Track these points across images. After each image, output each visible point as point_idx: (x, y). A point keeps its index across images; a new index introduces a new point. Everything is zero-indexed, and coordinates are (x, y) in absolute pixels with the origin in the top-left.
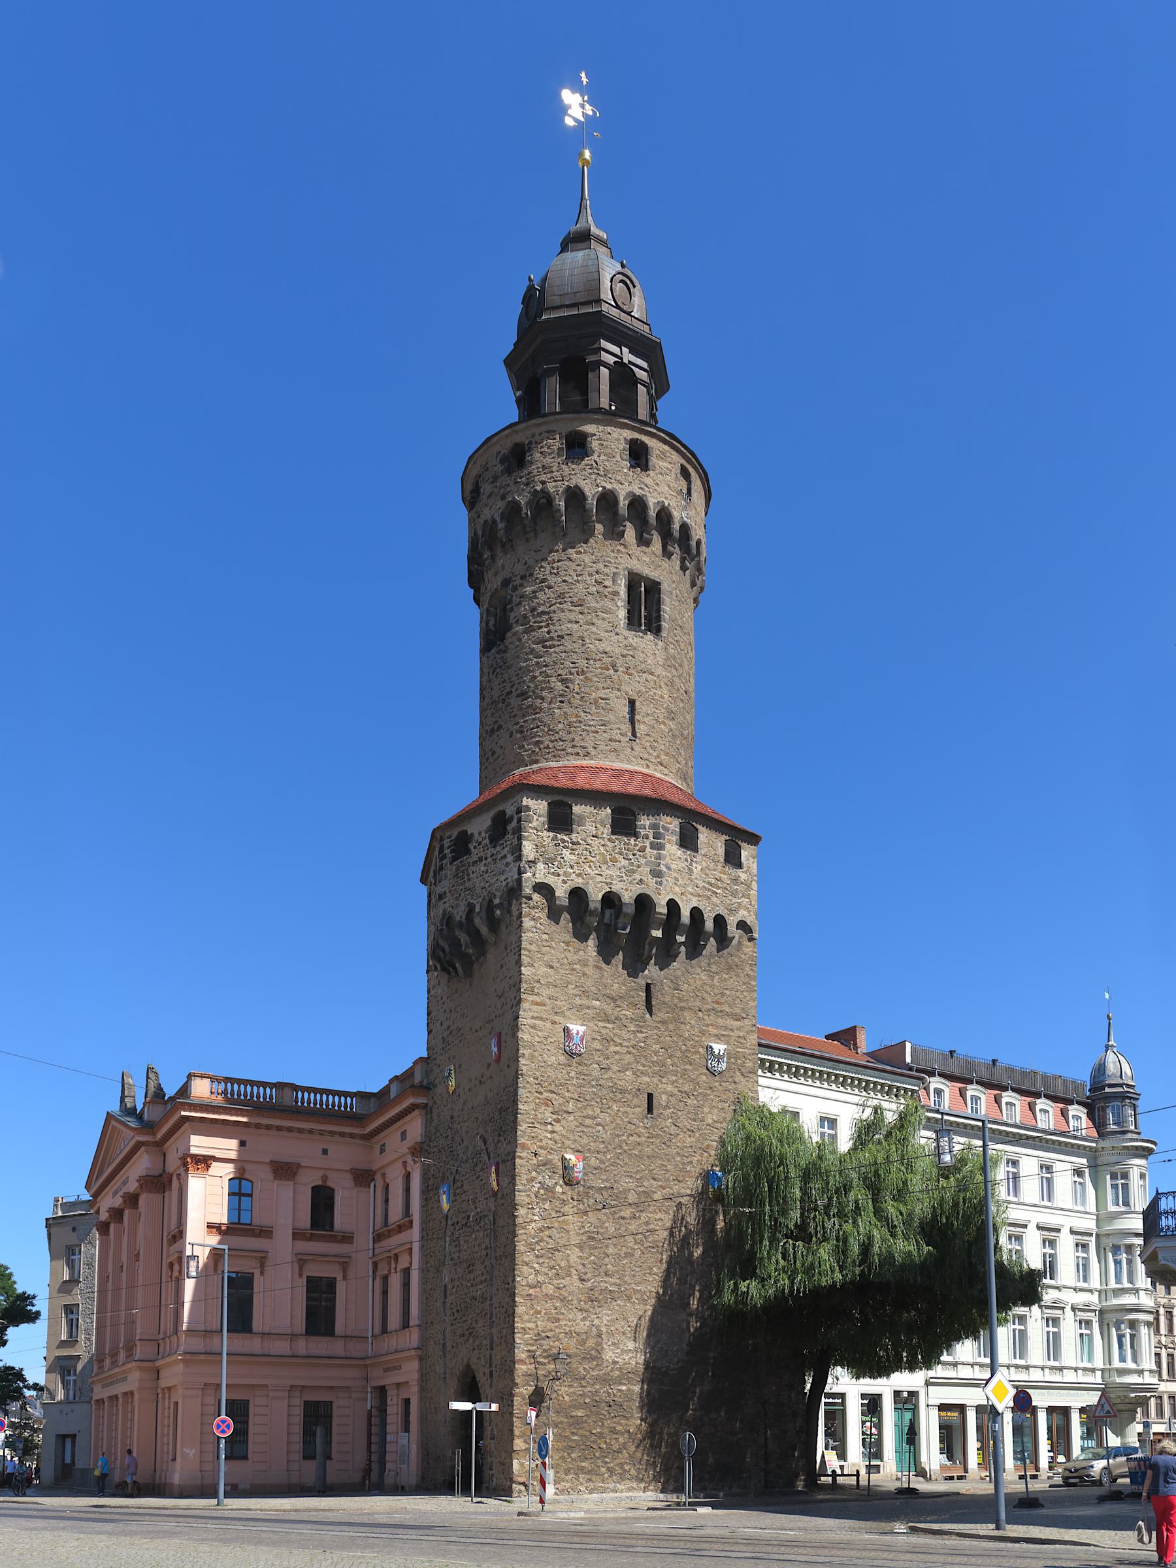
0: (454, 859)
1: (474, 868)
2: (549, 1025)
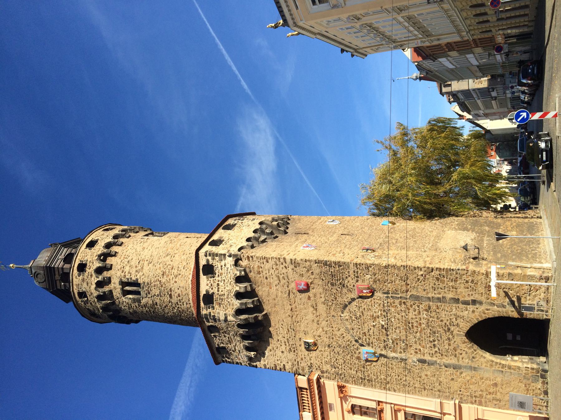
0: (213, 308)
1: (220, 290)
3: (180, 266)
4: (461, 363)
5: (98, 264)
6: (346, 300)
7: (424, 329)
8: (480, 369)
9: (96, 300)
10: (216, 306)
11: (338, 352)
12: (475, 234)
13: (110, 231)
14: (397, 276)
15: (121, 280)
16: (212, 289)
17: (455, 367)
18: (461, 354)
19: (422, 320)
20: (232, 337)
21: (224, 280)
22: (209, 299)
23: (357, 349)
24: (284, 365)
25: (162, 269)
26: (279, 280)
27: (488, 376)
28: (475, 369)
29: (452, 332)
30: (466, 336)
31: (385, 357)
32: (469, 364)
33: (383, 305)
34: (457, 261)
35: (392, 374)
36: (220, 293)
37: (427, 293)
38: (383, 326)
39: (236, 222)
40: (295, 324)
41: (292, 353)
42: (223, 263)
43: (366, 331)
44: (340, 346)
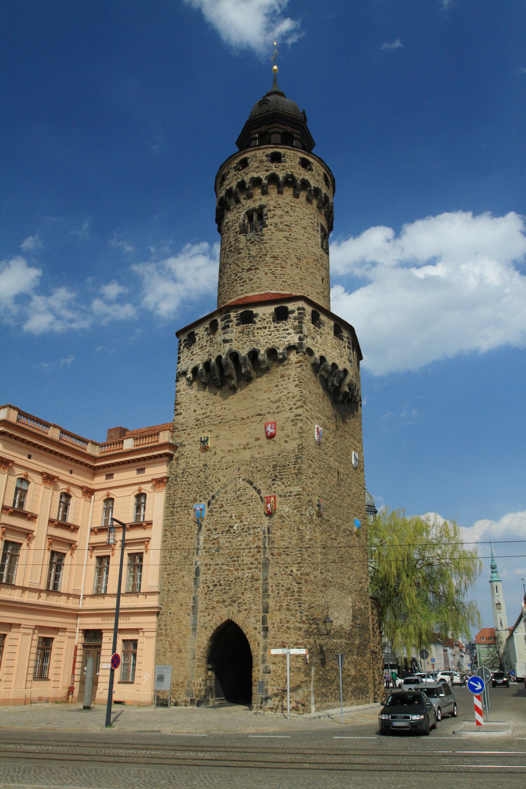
0: (238, 325)
1: (259, 331)
2: (310, 424)
3: (286, 276)
4: (199, 614)
5: (281, 175)
6: (257, 484)
7: (232, 574)
8: (195, 635)
9: (240, 180)
10: (240, 328)
11: (199, 476)
12: (348, 628)
13: (324, 183)
14: (290, 543)
15: (265, 206)
16: (260, 321)
17: (194, 608)
18: (209, 615)
19: (242, 572)
20: (207, 350)
21: (271, 335)
22: (247, 318)
23: (205, 499)
24: (181, 414)
25: (281, 255)
26: (275, 402)
27: (188, 643)
28: (194, 629)
29: (232, 605)
30: (229, 620)
31: (200, 529)
32: (198, 623)
33: (255, 528)
34: (311, 610)
35: (181, 539)
36: (256, 331)
37: (271, 577)
38: (232, 527)
39: (345, 339)
40: (227, 424)
41: (194, 422)
42: (291, 331)
43: (225, 508)
44: (206, 478)
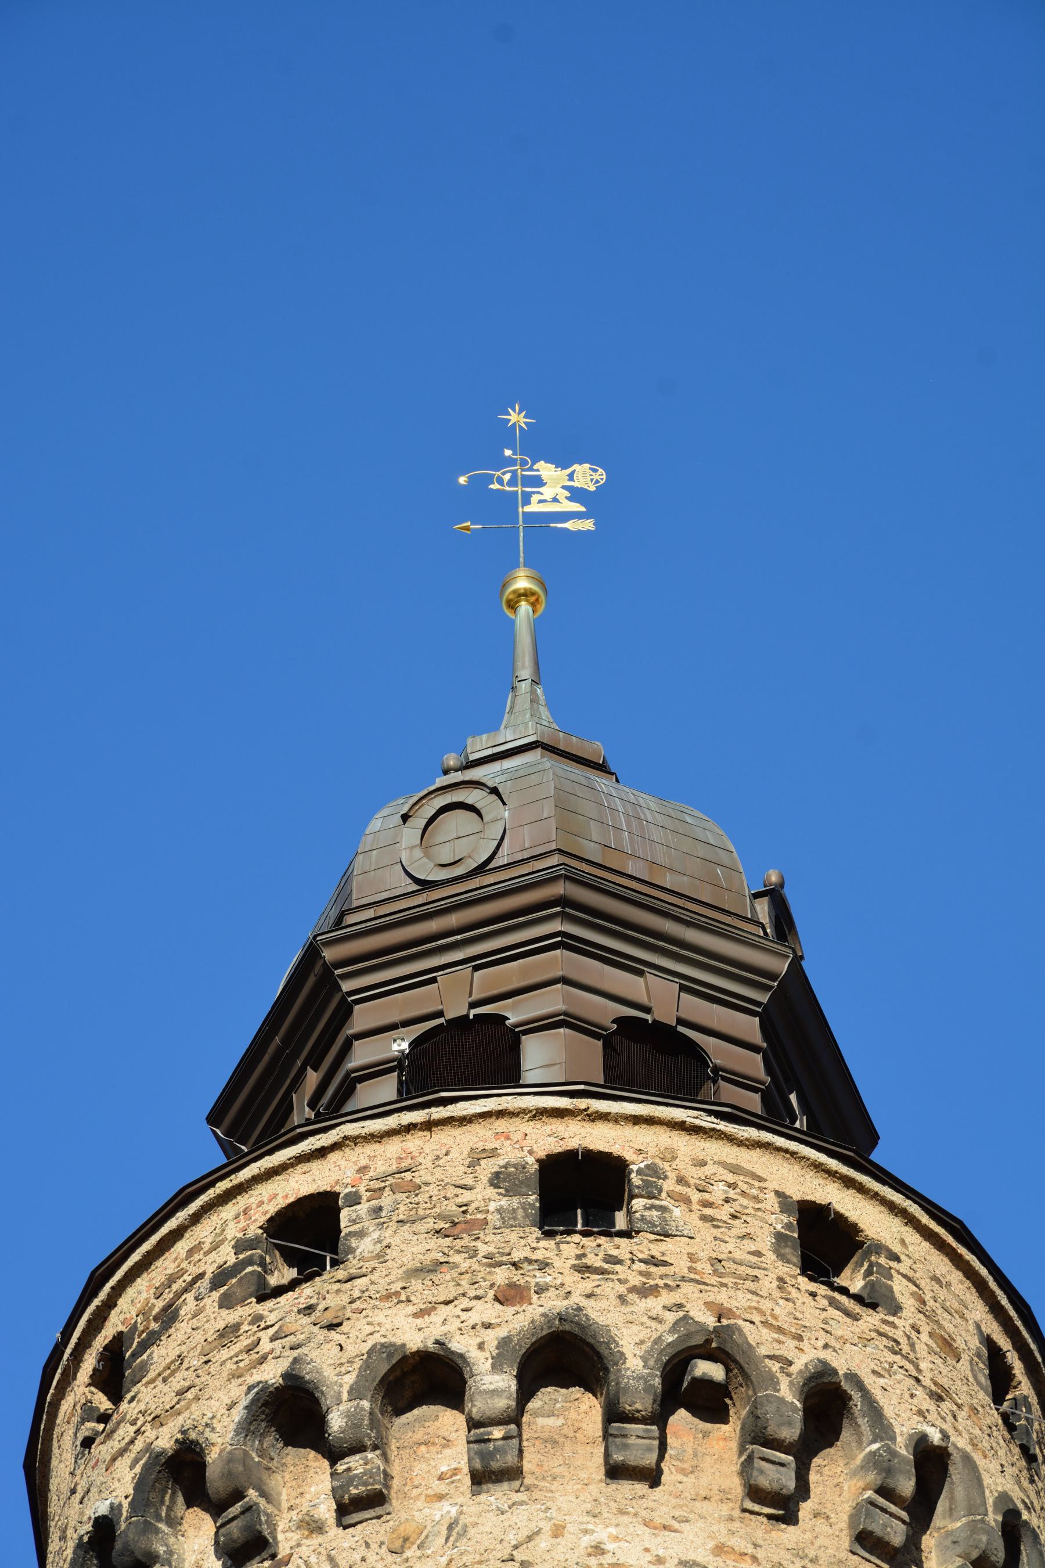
9: (272, 1373)
